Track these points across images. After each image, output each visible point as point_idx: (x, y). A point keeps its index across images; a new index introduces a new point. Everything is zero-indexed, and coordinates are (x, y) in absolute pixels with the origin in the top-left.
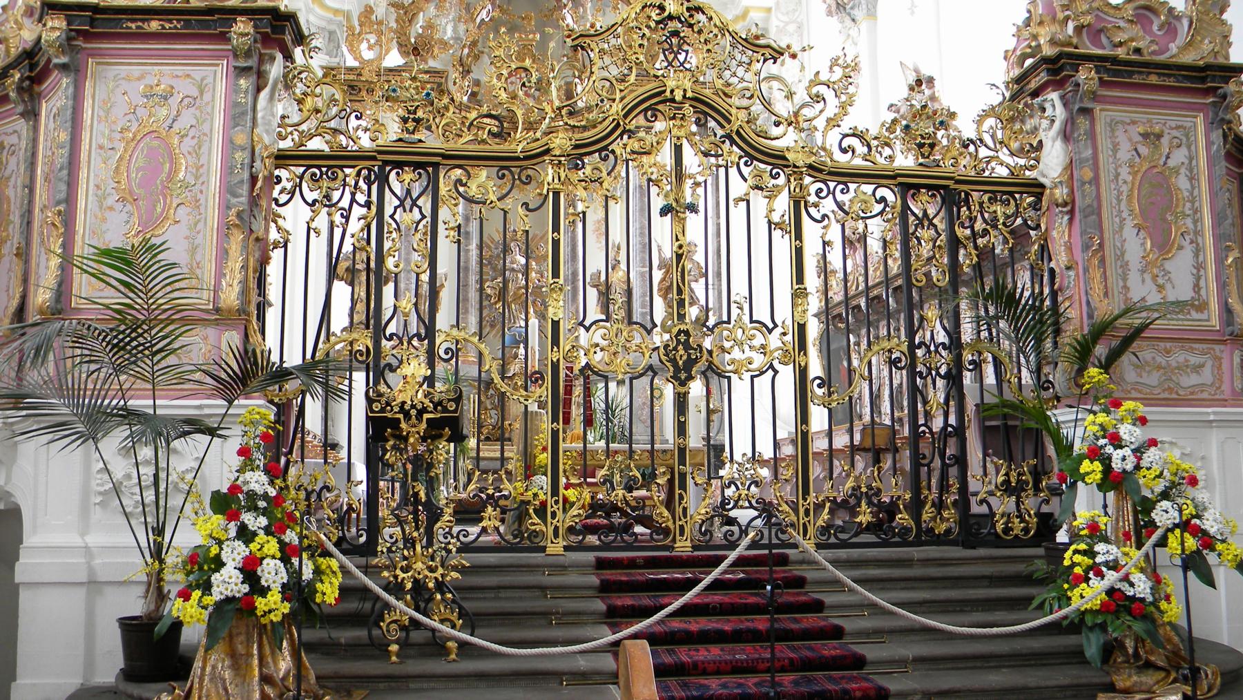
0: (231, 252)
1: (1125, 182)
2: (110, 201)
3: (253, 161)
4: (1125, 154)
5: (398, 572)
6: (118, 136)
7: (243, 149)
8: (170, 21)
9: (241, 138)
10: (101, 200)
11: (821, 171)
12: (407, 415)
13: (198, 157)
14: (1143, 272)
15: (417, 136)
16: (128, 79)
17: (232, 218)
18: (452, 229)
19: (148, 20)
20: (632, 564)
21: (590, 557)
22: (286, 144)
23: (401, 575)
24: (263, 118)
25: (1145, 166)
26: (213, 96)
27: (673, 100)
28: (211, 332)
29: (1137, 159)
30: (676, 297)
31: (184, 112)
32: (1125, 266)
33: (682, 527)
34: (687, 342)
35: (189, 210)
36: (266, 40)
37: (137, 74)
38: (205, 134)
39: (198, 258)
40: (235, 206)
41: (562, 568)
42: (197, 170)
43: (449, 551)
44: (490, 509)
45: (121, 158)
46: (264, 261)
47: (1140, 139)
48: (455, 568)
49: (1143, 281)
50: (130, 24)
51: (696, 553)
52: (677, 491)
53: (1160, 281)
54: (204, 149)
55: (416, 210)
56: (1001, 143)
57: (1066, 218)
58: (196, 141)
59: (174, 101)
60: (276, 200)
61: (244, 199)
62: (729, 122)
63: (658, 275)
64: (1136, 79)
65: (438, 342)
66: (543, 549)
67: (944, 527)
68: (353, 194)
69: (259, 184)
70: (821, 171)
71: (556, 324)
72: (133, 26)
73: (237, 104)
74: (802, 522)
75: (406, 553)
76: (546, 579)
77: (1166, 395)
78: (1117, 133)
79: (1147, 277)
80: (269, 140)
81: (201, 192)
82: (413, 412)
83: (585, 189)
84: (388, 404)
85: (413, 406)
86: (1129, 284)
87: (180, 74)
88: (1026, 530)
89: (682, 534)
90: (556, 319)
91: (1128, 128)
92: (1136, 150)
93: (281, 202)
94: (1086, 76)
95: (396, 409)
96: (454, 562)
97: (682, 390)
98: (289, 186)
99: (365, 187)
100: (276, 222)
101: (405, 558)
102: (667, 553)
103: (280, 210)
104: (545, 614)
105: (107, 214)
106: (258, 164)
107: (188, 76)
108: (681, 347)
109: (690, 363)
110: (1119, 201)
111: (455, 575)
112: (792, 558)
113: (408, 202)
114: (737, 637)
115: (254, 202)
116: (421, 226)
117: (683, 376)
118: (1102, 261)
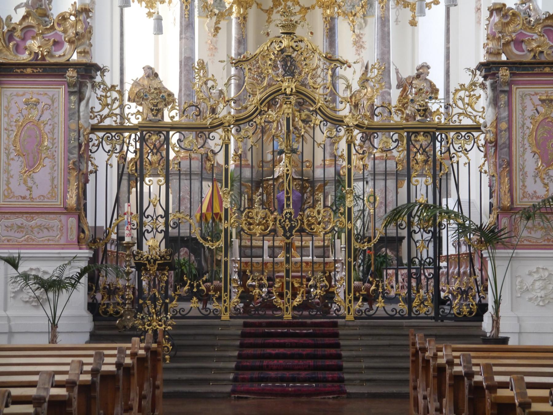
0: (71, 181)
1: (528, 128)
2: (12, 156)
3: (79, 136)
4: (529, 112)
5: (146, 326)
6: (14, 124)
7: (75, 131)
8: (36, 69)
9: (74, 126)
10: (8, 155)
11: (362, 127)
12: (149, 261)
13: (53, 134)
14: (535, 177)
15: (157, 118)
16: (17, 95)
17: (71, 166)
18: (176, 164)
19: (26, 68)
20: (260, 325)
21: (241, 321)
22: (95, 121)
23: (147, 328)
24: (83, 115)
25: (542, 118)
26: (59, 104)
27: (286, 94)
28: (63, 218)
29: (537, 115)
30: (286, 195)
31: (45, 112)
32: (525, 175)
33: (287, 308)
34: (290, 218)
35: (50, 160)
36: (82, 76)
37: (21, 93)
38: (56, 123)
39: (55, 183)
40: (72, 159)
41: (226, 326)
42: (53, 141)
43: (167, 318)
44: (195, 298)
45: (16, 135)
46: (87, 181)
47: (540, 103)
48: (169, 325)
49: (535, 182)
50: (17, 70)
51: (295, 320)
52: (285, 291)
53: (546, 181)
54: (56, 131)
55: (159, 154)
56: (468, 104)
57: (493, 149)
58: (51, 126)
59: (40, 106)
60: (91, 151)
61: (76, 156)
62: (315, 103)
63: (395, 94)
64: (536, 71)
65: (170, 219)
66: (220, 318)
67: (425, 309)
68: (128, 147)
69: (83, 148)
70: (362, 127)
71: (226, 210)
72: (19, 71)
73: (70, 109)
74: (347, 306)
75: (149, 318)
76: (219, 331)
77: (546, 243)
78: (525, 101)
79: (538, 179)
80: (85, 122)
81: (55, 151)
82: (152, 261)
83: (241, 141)
84: (141, 257)
85: (151, 258)
86: (526, 184)
87: (42, 93)
88: (470, 312)
89: (287, 311)
90: (226, 208)
91: (532, 97)
92: (537, 110)
93: (93, 151)
94: (504, 73)
95: (145, 260)
96: (169, 322)
97: (288, 241)
98: (97, 142)
99: (134, 144)
100: (91, 161)
101: (149, 321)
102: (280, 320)
103: (92, 155)
104: (213, 346)
105: (11, 162)
106: (82, 138)
107: (46, 94)
108: (287, 220)
109: (292, 228)
110: (523, 138)
111: (169, 327)
112: (339, 323)
113: (155, 151)
114: (292, 357)
115: (80, 156)
116: (161, 162)
117: (288, 234)
118: (510, 173)
